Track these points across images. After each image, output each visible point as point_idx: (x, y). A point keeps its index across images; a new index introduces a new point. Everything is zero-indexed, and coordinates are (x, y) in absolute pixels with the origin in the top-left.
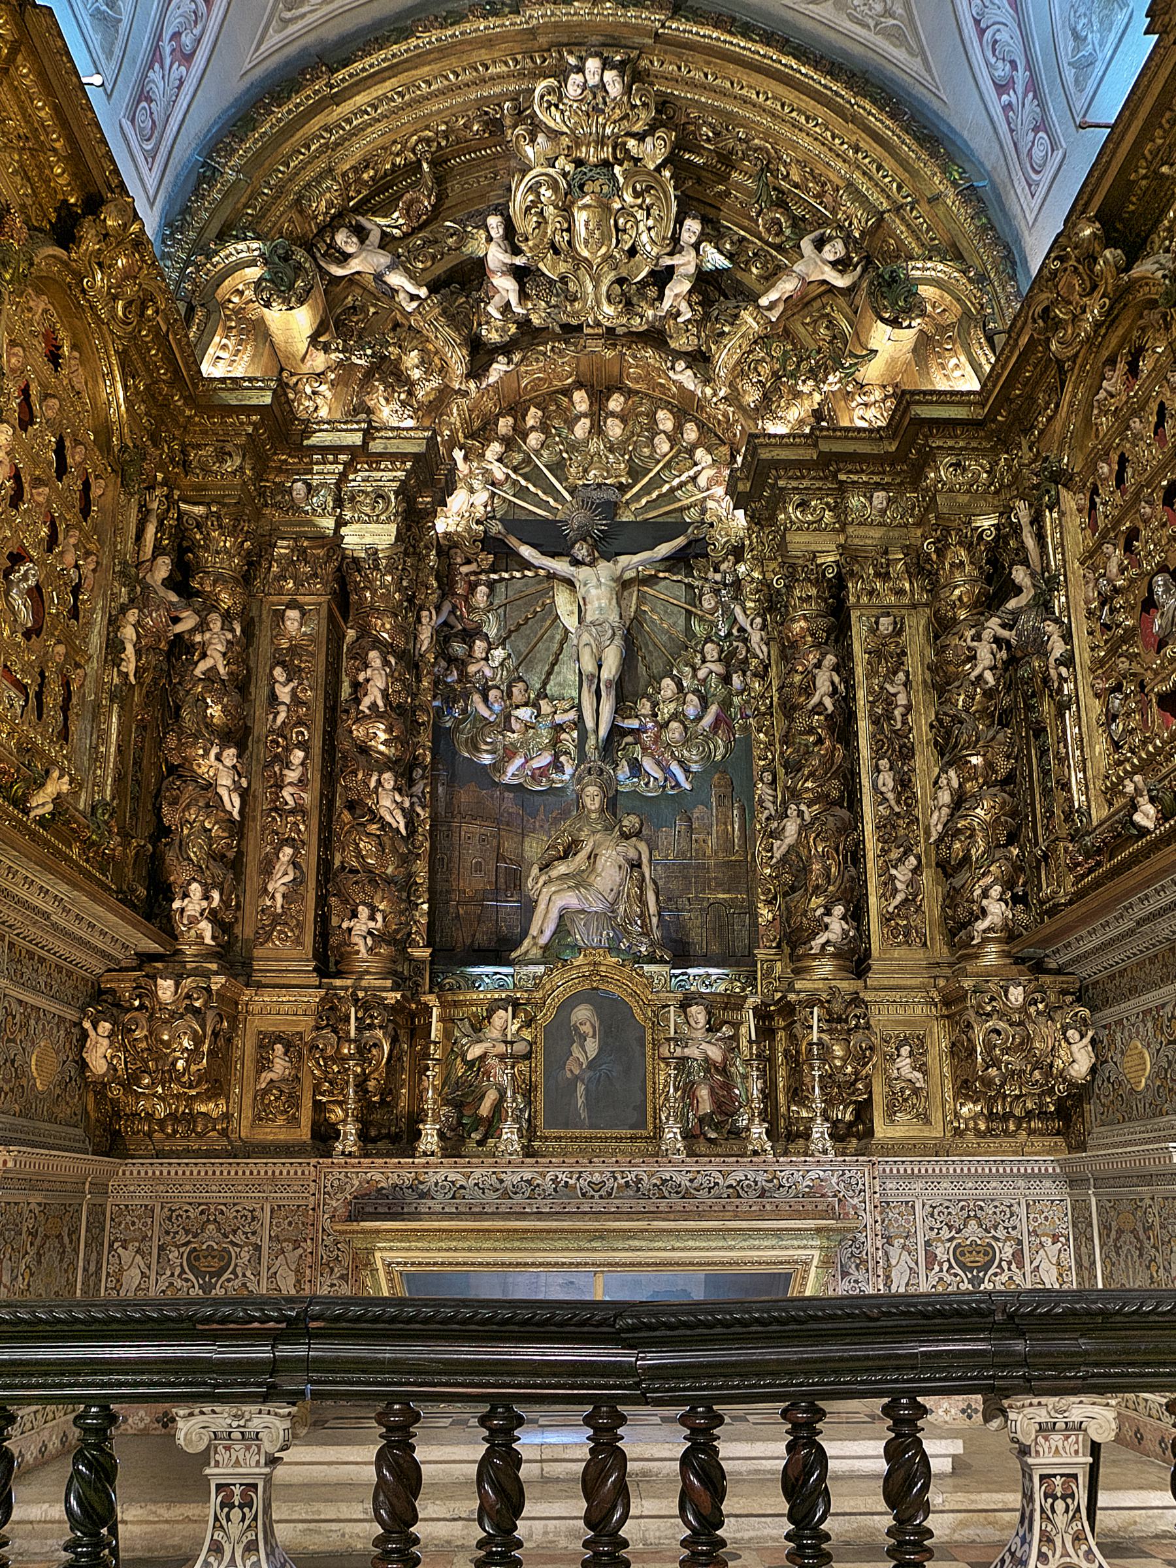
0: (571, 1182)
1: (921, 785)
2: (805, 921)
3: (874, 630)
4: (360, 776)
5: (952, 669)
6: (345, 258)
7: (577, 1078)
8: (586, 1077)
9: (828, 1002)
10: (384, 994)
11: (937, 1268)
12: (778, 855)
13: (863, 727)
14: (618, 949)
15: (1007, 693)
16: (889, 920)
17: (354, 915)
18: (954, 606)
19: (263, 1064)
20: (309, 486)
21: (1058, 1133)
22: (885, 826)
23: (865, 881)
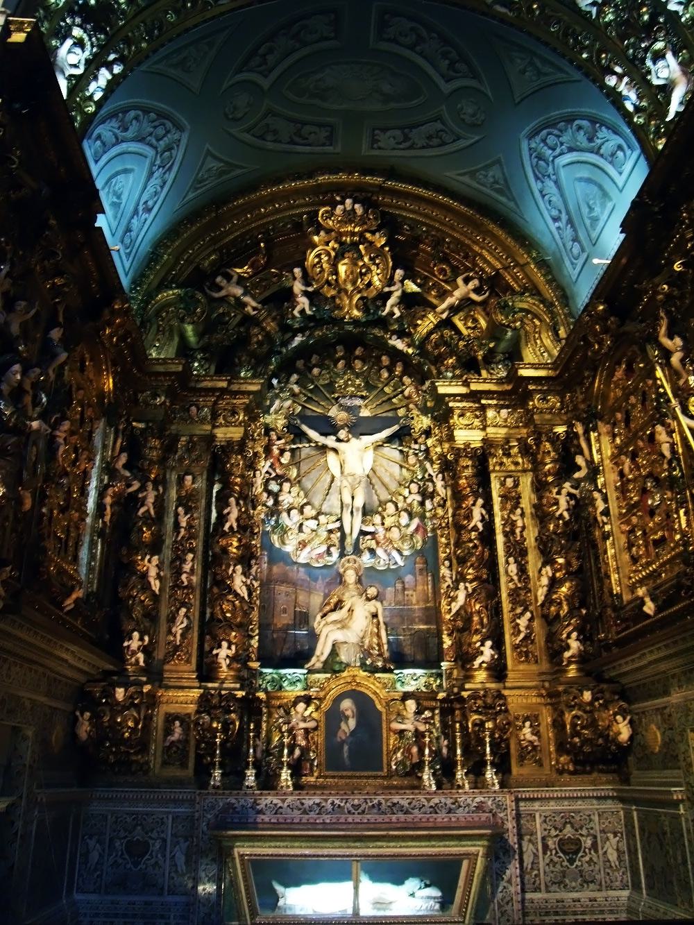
0: (342, 805)
1: (532, 570)
2: (470, 650)
3: (503, 484)
4: (224, 567)
6: (220, 288)
7: (343, 742)
8: (349, 741)
9: (484, 696)
10: (236, 693)
11: (549, 853)
12: (454, 611)
13: (500, 539)
15: (576, 523)
16: (517, 648)
17: (220, 646)
19: (168, 731)
20: (198, 409)
21: (614, 772)
22: (512, 595)
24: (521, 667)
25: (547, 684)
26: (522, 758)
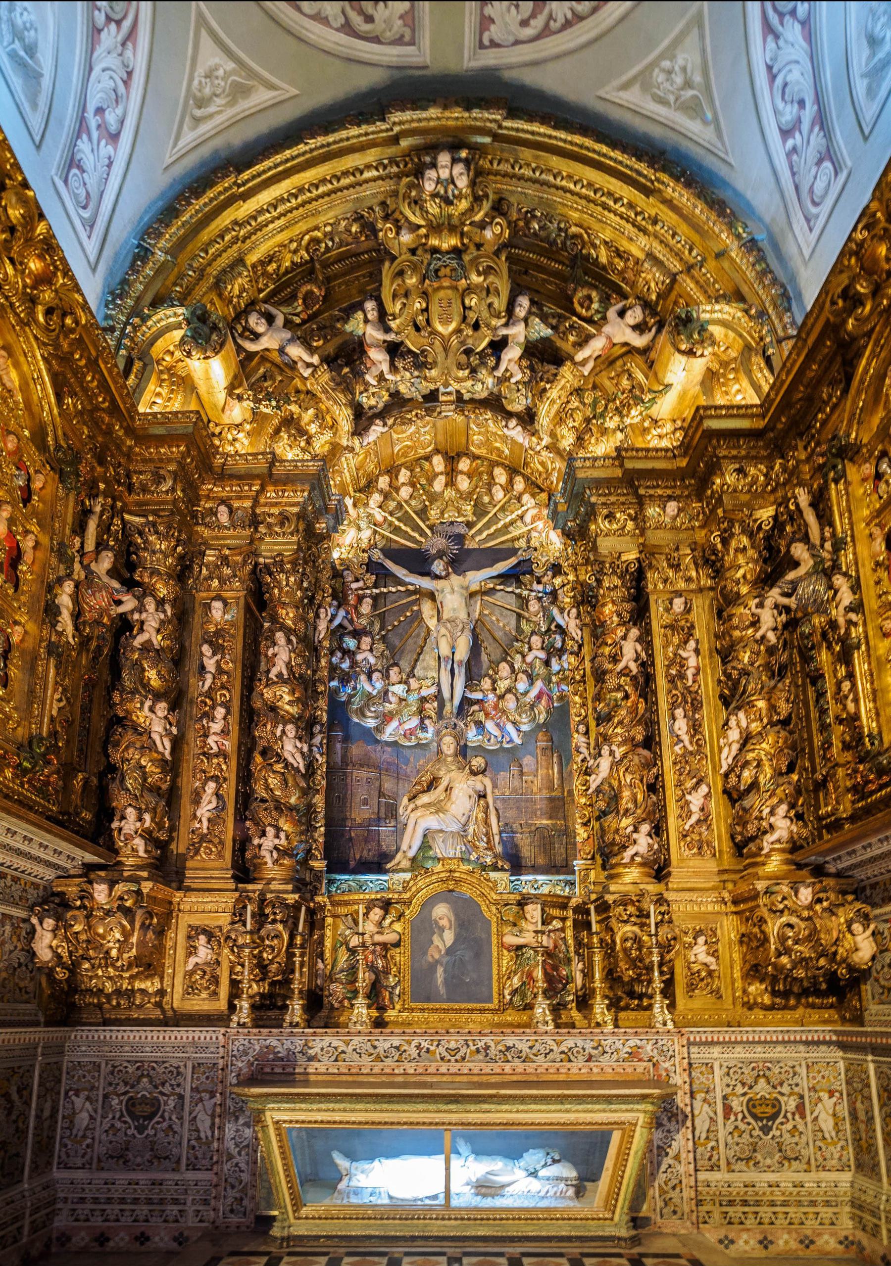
5: (737, 633)
7: (437, 962)
14: (469, 860)
16: (685, 836)
17: (263, 834)
18: (738, 582)
23: (665, 806)
24: (691, 863)
25: (730, 886)
26: (691, 987)
